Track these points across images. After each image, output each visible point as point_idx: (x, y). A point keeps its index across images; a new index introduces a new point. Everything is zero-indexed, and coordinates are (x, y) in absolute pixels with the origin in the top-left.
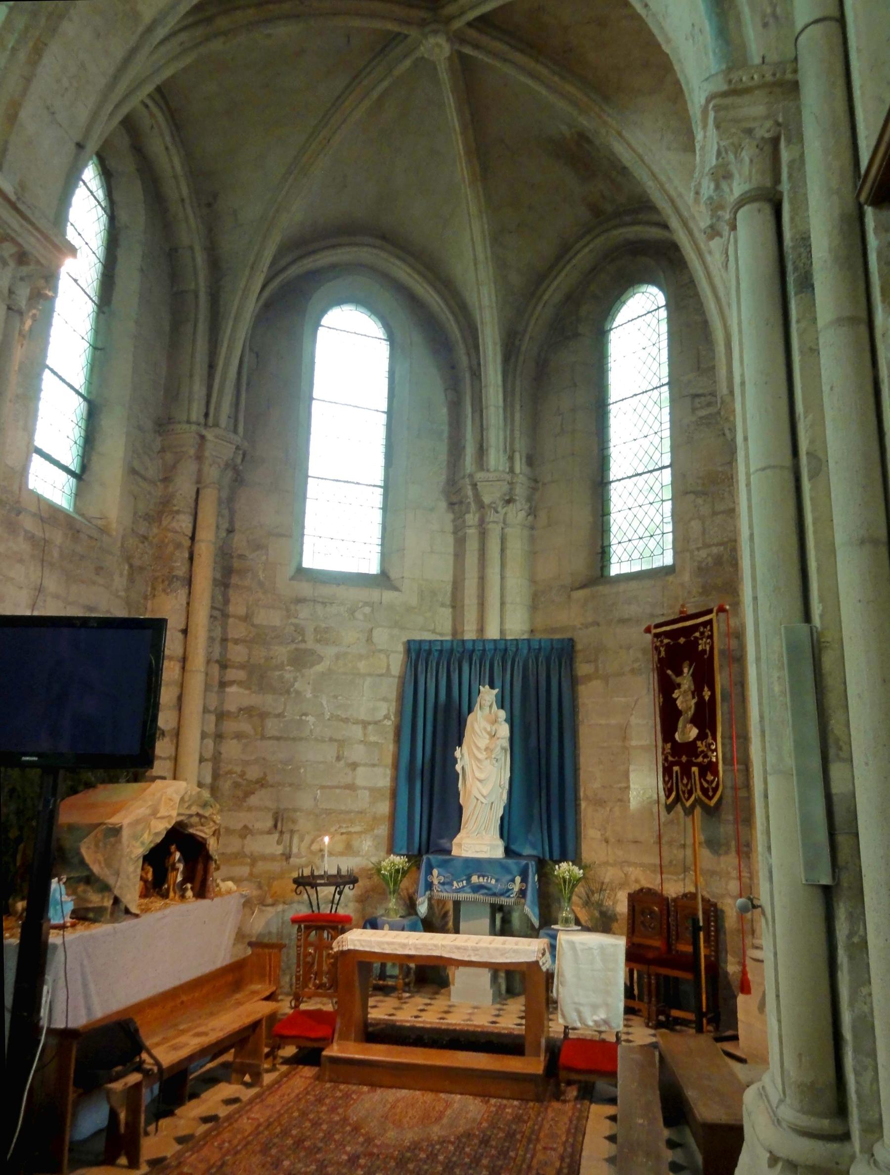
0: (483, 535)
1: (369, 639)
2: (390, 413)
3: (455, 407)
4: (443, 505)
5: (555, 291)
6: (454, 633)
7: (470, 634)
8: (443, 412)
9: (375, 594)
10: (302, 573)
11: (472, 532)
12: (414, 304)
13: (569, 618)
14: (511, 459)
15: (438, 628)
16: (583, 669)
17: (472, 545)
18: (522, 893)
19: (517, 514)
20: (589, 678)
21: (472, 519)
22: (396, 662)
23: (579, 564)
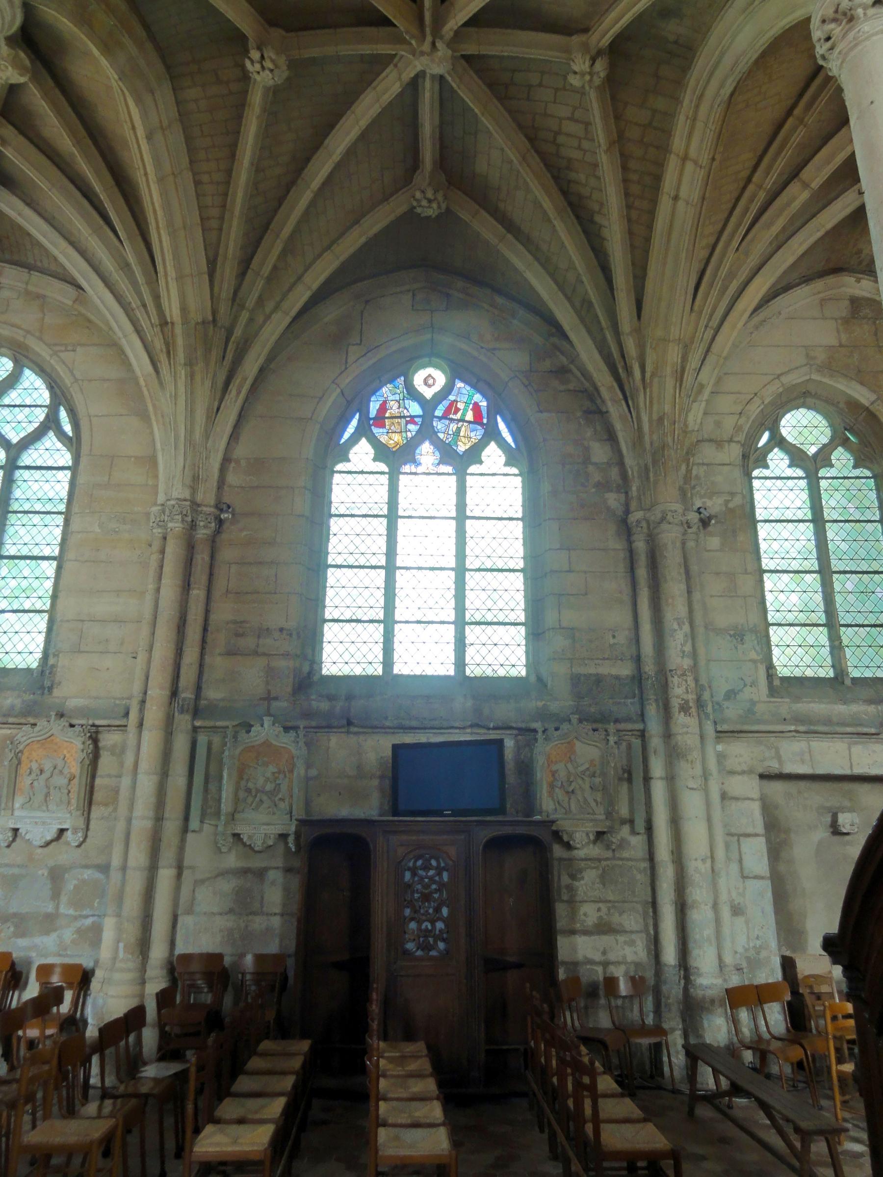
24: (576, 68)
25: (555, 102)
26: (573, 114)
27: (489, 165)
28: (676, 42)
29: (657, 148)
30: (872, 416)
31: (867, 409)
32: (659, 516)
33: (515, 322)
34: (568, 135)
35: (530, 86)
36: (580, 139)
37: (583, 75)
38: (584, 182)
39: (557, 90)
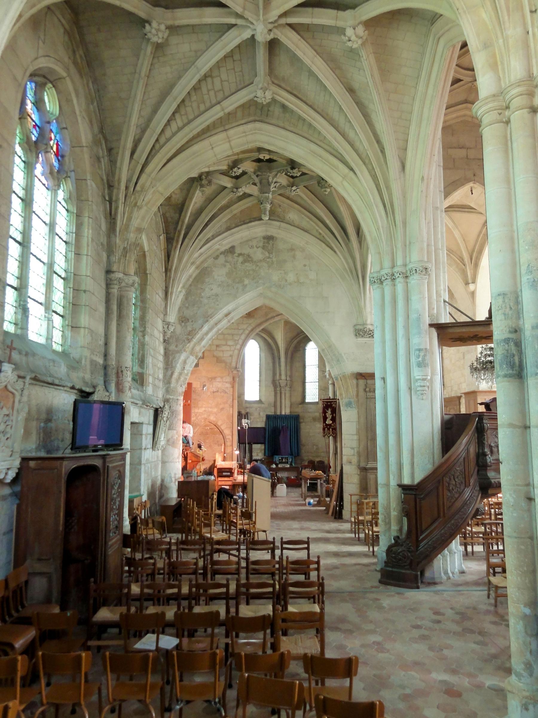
0: (281, 393)
1: (259, 414)
2: (260, 364)
3: (274, 363)
4: (272, 385)
5: (295, 342)
6: (275, 412)
7: (278, 413)
8: (271, 365)
9: (260, 405)
10: (247, 402)
11: (278, 392)
12: (265, 340)
13: (298, 410)
14: (286, 376)
15: (271, 412)
16: (301, 420)
17: (279, 395)
18: (292, 462)
19: (288, 389)
20: (302, 422)
21: (278, 389)
22: (264, 419)
23: (299, 399)
24: (267, 93)
25: (227, 70)
26: (225, 81)
27: (177, 44)
28: (268, 110)
29: (221, 122)
30: (144, 256)
31: (145, 252)
32: (131, 282)
33: (91, 106)
34: (213, 83)
35: (232, 56)
36: (214, 89)
37: (265, 98)
38: (192, 100)
39: (234, 69)
